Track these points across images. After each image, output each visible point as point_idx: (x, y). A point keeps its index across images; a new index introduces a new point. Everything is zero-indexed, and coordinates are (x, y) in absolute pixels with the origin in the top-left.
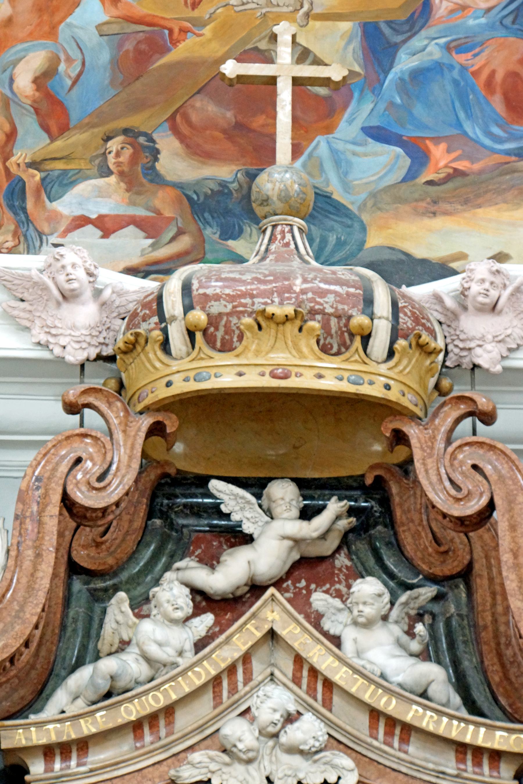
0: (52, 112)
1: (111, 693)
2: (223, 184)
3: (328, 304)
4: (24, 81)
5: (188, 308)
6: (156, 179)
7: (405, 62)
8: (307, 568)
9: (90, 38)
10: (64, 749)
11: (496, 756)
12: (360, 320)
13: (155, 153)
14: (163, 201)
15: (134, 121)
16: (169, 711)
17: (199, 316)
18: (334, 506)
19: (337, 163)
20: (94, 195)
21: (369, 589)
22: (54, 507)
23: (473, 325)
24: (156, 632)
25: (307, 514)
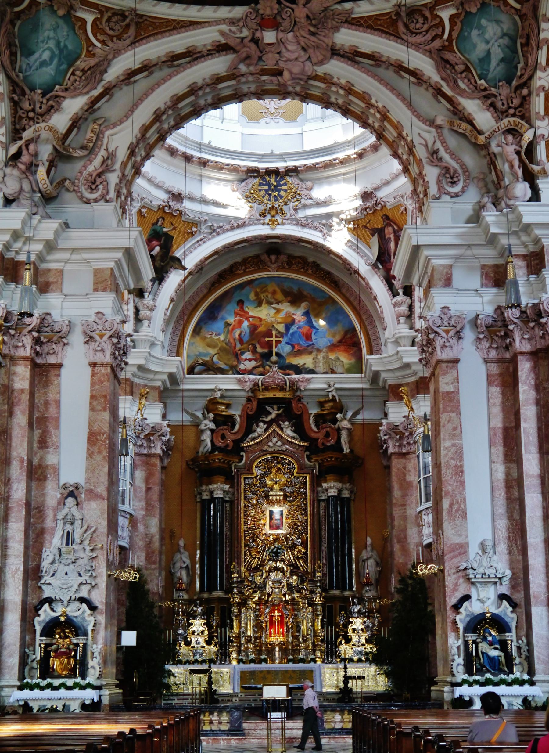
1: (254, 439)
4: (237, 336)
7: (291, 331)
8: (278, 415)
9: (246, 328)
10: (248, 446)
13: (256, 347)
14: (258, 356)
15: (253, 342)
16: (261, 441)
20: (247, 355)
21: (287, 423)
23: (300, 383)
24: (260, 429)
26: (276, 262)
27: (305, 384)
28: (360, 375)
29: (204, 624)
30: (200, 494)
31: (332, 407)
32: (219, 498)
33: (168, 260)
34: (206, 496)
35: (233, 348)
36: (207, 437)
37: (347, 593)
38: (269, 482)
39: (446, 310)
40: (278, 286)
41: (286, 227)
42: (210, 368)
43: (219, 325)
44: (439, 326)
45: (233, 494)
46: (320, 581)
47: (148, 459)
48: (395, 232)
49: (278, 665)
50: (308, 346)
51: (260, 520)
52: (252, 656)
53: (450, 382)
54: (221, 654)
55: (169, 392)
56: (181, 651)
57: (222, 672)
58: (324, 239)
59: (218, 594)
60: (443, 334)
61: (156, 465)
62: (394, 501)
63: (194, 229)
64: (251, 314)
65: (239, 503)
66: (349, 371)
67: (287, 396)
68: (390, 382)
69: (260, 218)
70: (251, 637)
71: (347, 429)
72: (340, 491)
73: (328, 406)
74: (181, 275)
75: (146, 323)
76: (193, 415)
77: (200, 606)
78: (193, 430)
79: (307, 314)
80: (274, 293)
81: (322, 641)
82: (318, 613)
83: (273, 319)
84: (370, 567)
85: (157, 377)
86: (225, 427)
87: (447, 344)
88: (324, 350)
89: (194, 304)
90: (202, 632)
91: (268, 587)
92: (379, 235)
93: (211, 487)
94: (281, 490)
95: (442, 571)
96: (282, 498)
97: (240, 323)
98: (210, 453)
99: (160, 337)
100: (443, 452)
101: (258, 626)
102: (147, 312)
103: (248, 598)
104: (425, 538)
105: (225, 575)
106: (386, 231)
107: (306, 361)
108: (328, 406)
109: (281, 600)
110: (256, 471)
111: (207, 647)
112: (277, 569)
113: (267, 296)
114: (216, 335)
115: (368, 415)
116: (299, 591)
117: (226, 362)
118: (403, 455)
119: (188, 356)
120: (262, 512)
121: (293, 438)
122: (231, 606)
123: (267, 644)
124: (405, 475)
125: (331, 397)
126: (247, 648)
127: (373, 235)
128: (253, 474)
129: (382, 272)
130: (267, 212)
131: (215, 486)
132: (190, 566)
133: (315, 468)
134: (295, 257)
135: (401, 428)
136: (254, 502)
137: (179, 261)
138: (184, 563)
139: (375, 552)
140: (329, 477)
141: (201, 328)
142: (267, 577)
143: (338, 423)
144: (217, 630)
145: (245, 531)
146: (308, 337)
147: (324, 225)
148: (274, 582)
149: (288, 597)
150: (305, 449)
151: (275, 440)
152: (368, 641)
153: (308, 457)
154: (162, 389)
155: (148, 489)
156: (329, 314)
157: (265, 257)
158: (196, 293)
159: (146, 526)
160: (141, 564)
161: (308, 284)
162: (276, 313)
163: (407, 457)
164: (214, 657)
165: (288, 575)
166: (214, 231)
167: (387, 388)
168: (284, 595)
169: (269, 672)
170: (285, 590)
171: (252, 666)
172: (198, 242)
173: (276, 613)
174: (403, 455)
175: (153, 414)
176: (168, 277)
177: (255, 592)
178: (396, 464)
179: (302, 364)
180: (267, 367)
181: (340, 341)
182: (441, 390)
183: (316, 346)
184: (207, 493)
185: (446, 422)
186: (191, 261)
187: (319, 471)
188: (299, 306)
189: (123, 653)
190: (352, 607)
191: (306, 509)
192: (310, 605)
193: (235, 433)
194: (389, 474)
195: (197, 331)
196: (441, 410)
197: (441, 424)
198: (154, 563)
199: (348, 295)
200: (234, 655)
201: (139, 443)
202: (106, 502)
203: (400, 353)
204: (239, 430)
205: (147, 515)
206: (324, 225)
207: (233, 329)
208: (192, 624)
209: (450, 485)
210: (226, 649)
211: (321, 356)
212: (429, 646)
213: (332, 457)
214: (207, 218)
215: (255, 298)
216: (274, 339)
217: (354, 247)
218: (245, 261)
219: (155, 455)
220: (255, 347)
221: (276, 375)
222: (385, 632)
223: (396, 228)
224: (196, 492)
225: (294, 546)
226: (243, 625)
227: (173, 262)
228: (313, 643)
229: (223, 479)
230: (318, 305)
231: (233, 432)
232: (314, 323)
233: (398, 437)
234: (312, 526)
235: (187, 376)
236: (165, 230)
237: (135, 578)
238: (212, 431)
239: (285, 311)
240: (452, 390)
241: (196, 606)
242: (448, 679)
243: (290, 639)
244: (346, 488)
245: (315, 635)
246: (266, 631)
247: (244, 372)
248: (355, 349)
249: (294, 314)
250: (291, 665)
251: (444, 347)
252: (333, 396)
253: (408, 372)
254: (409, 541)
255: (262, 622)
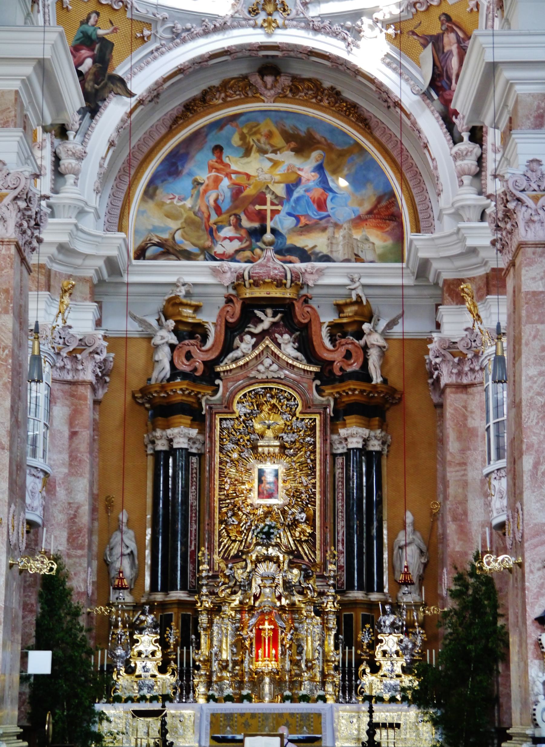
0: (218, 209)
1: (236, 360)
2: (256, 228)
3: (278, 277)
4: (212, 202)
5: (250, 278)
6: (241, 226)
7: (295, 195)
8: (274, 324)
10: (227, 371)
11: (311, 372)
12: (284, 281)
13: (240, 220)
14: (243, 233)
15: (236, 211)
16: (247, 363)
17: (252, 281)
18: (279, 315)
19: (280, 222)
20: (228, 231)
21: (286, 336)
22: (223, 323)
23: (307, 276)
24: (245, 345)
25: (274, 316)
26: (273, 86)
27: (315, 277)
28: (399, 265)
29: (156, 641)
30: (153, 442)
31: (356, 314)
32: (182, 449)
33: (106, 80)
34: (162, 446)
35: (205, 220)
36: (163, 356)
37: (375, 597)
38: (258, 426)
39: (535, 166)
40: (276, 123)
41: (289, 31)
42: (168, 250)
43: (183, 184)
44: (524, 190)
45: (204, 444)
46: (334, 577)
47: (74, 388)
48: (459, 41)
49: (267, 705)
50: (321, 219)
51: (243, 484)
52: (229, 691)
53: (539, 277)
54: (181, 687)
55: (105, 285)
56: (120, 682)
57: (182, 716)
58: (349, 52)
59: (178, 595)
60: (529, 202)
61: (85, 399)
62: (449, 458)
63: (146, 32)
64: (234, 167)
65: (212, 458)
66: (383, 258)
67: (288, 296)
68: (445, 276)
69: (249, 16)
70: (227, 661)
71: (379, 347)
72: (366, 441)
73: (350, 311)
74: (125, 104)
75: (70, 179)
76: (142, 322)
77: (151, 612)
78: (144, 344)
79: (320, 169)
80: (270, 135)
81: (336, 668)
82: (331, 626)
83: (267, 176)
84: (411, 559)
85: (88, 262)
86: (192, 341)
87: (536, 218)
88: (345, 226)
89: (146, 150)
90: (153, 654)
91: (254, 585)
92: (434, 45)
93: (169, 432)
94: (277, 438)
95: (521, 565)
96: (277, 450)
97: (217, 181)
98: (169, 380)
99: (93, 201)
100: (525, 384)
101: (239, 644)
102: (73, 162)
103: (224, 601)
104: (495, 514)
105: (190, 567)
106: (446, 40)
107: (315, 241)
108: (350, 311)
109: (274, 607)
110: (239, 409)
111: (159, 676)
112: (268, 558)
113: (259, 141)
114: (180, 200)
115: (412, 327)
116: (301, 593)
117: (194, 241)
118: (464, 388)
119: (136, 232)
120: (247, 471)
121: (297, 359)
122: (197, 613)
123: (251, 672)
124: (465, 418)
125: (354, 298)
126: (221, 679)
127: (425, 46)
128: (234, 412)
129: (437, 104)
130: (260, 7)
131: (176, 431)
132: (135, 553)
133: (329, 405)
134: (303, 80)
135: (461, 347)
136: (235, 456)
137: (122, 81)
138: (127, 547)
139: (418, 534)
140: (350, 419)
141: (156, 189)
142: (253, 570)
143: (365, 337)
144: (175, 650)
145: (220, 500)
146: (321, 205)
147: (348, 29)
148: (263, 578)
149: (284, 602)
150: (313, 376)
151: (268, 362)
152: (406, 670)
153: (317, 386)
154: (95, 281)
155: (73, 434)
156: (353, 170)
157: (256, 79)
158: (150, 134)
159: (70, 491)
160: (60, 548)
161: (321, 122)
162: (272, 167)
163: (470, 390)
164: (170, 691)
165: (286, 568)
166: (178, 35)
167: (441, 284)
168: (279, 598)
169: (253, 716)
170: (280, 590)
171: (229, 707)
172: (152, 52)
173: (267, 626)
174: (464, 388)
175: (82, 321)
176: (106, 107)
177: (235, 593)
178: (453, 401)
179: (310, 246)
180: (258, 251)
181: (370, 212)
182: (524, 289)
183: (333, 220)
184: (164, 442)
185: (531, 338)
186: (141, 84)
187: (335, 411)
188: (308, 157)
189: (30, 685)
190: (382, 618)
191: (314, 467)
192: (318, 613)
193: (207, 351)
194: (442, 416)
195: (150, 193)
196: (524, 319)
197: (523, 341)
198: (81, 547)
199: (383, 140)
200: (201, 689)
201: (59, 364)
202: (7, 453)
203: (463, 231)
204: (213, 345)
205: (71, 474)
206: (348, 29)
207: (205, 191)
208: (137, 641)
209: (535, 434)
210: (188, 680)
211: (340, 235)
212: (500, 679)
213: (355, 390)
214: (166, 15)
215: (240, 143)
216: (268, 207)
217: (394, 66)
218: (225, 85)
219: (83, 383)
220: (239, 220)
221: (270, 263)
222: (432, 657)
223: (461, 35)
224: (146, 441)
225: (295, 523)
226: (215, 643)
227: (113, 83)
228: (322, 673)
229: (187, 420)
230: (338, 156)
231: (204, 348)
232: (331, 184)
233: (456, 360)
234: (324, 493)
235: (135, 262)
236: (100, 32)
237: (51, 569)
238: (172, 347)
239: (287, 163)
240: (541, 289)
241: (143, 613)
242: (529, 732)
243: (288, 666)
244: (376, 437)
245: (326, 661)
246: (251, 652)
247: (222, 257)
248: (393, 224)
249: (299, 169)
250: (288, 704)
251: (530, 221)
252: (358, 296)
253: (473, 260)
254: (470, 518)
255: (244, 639)
